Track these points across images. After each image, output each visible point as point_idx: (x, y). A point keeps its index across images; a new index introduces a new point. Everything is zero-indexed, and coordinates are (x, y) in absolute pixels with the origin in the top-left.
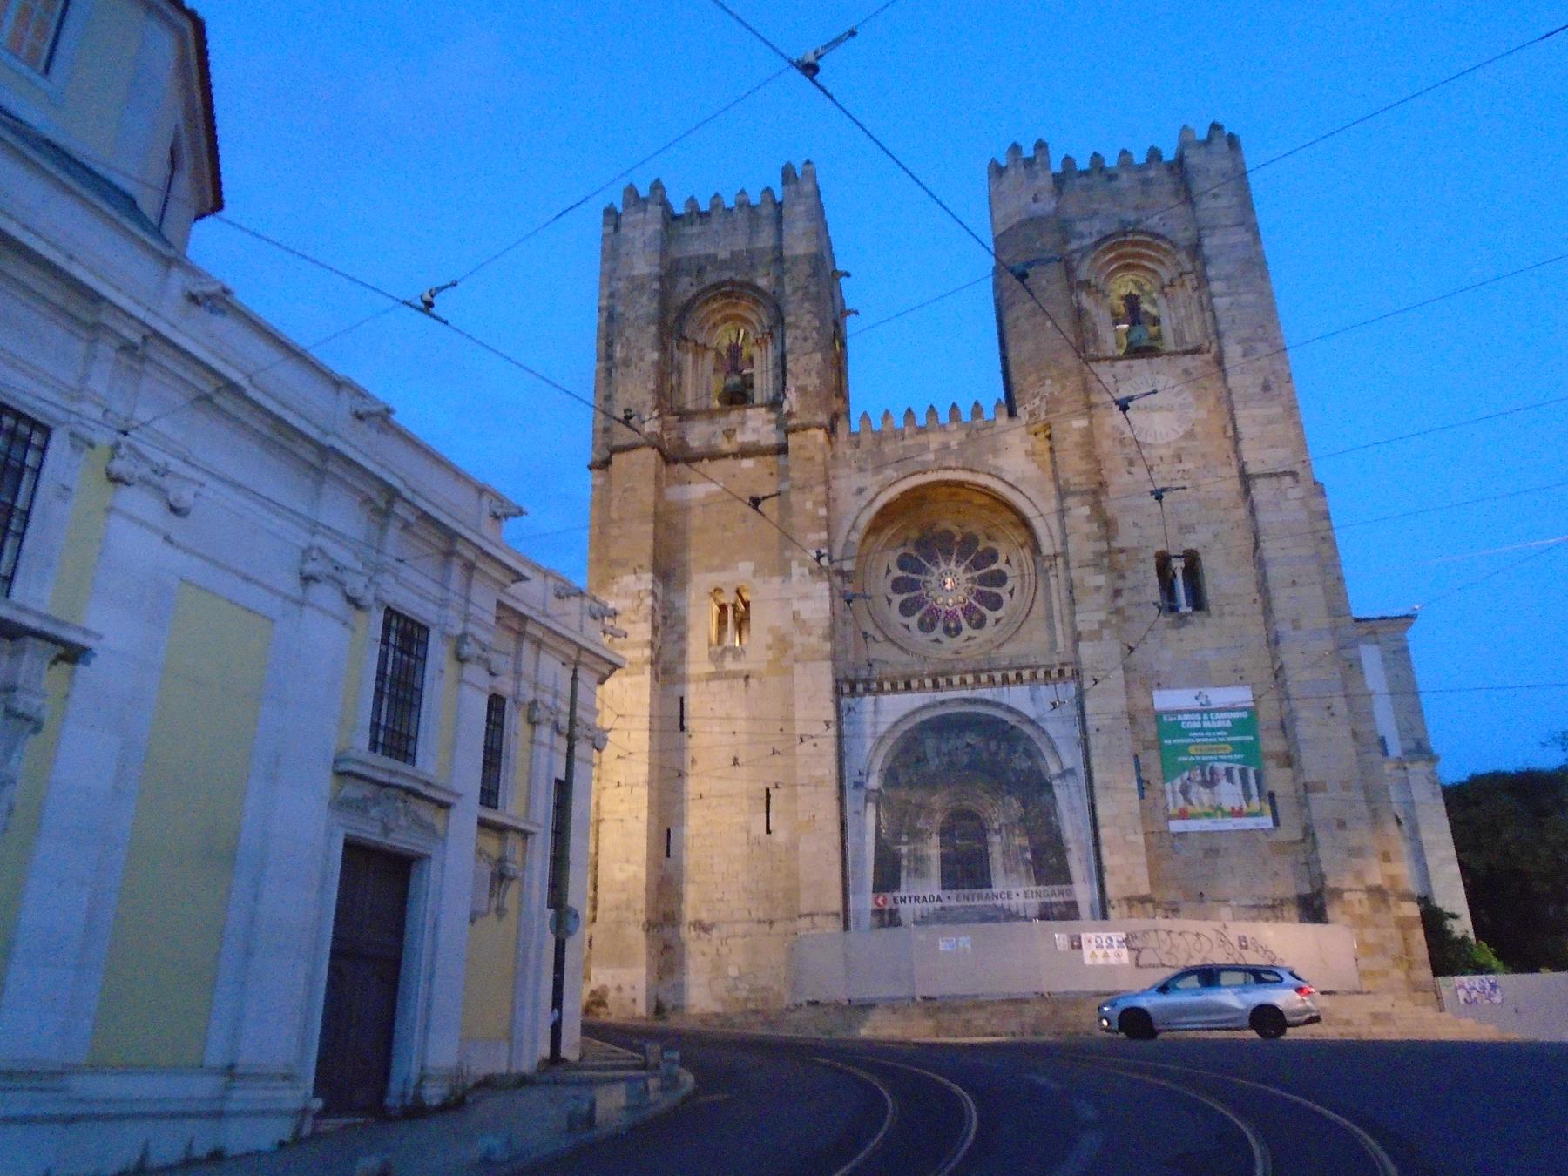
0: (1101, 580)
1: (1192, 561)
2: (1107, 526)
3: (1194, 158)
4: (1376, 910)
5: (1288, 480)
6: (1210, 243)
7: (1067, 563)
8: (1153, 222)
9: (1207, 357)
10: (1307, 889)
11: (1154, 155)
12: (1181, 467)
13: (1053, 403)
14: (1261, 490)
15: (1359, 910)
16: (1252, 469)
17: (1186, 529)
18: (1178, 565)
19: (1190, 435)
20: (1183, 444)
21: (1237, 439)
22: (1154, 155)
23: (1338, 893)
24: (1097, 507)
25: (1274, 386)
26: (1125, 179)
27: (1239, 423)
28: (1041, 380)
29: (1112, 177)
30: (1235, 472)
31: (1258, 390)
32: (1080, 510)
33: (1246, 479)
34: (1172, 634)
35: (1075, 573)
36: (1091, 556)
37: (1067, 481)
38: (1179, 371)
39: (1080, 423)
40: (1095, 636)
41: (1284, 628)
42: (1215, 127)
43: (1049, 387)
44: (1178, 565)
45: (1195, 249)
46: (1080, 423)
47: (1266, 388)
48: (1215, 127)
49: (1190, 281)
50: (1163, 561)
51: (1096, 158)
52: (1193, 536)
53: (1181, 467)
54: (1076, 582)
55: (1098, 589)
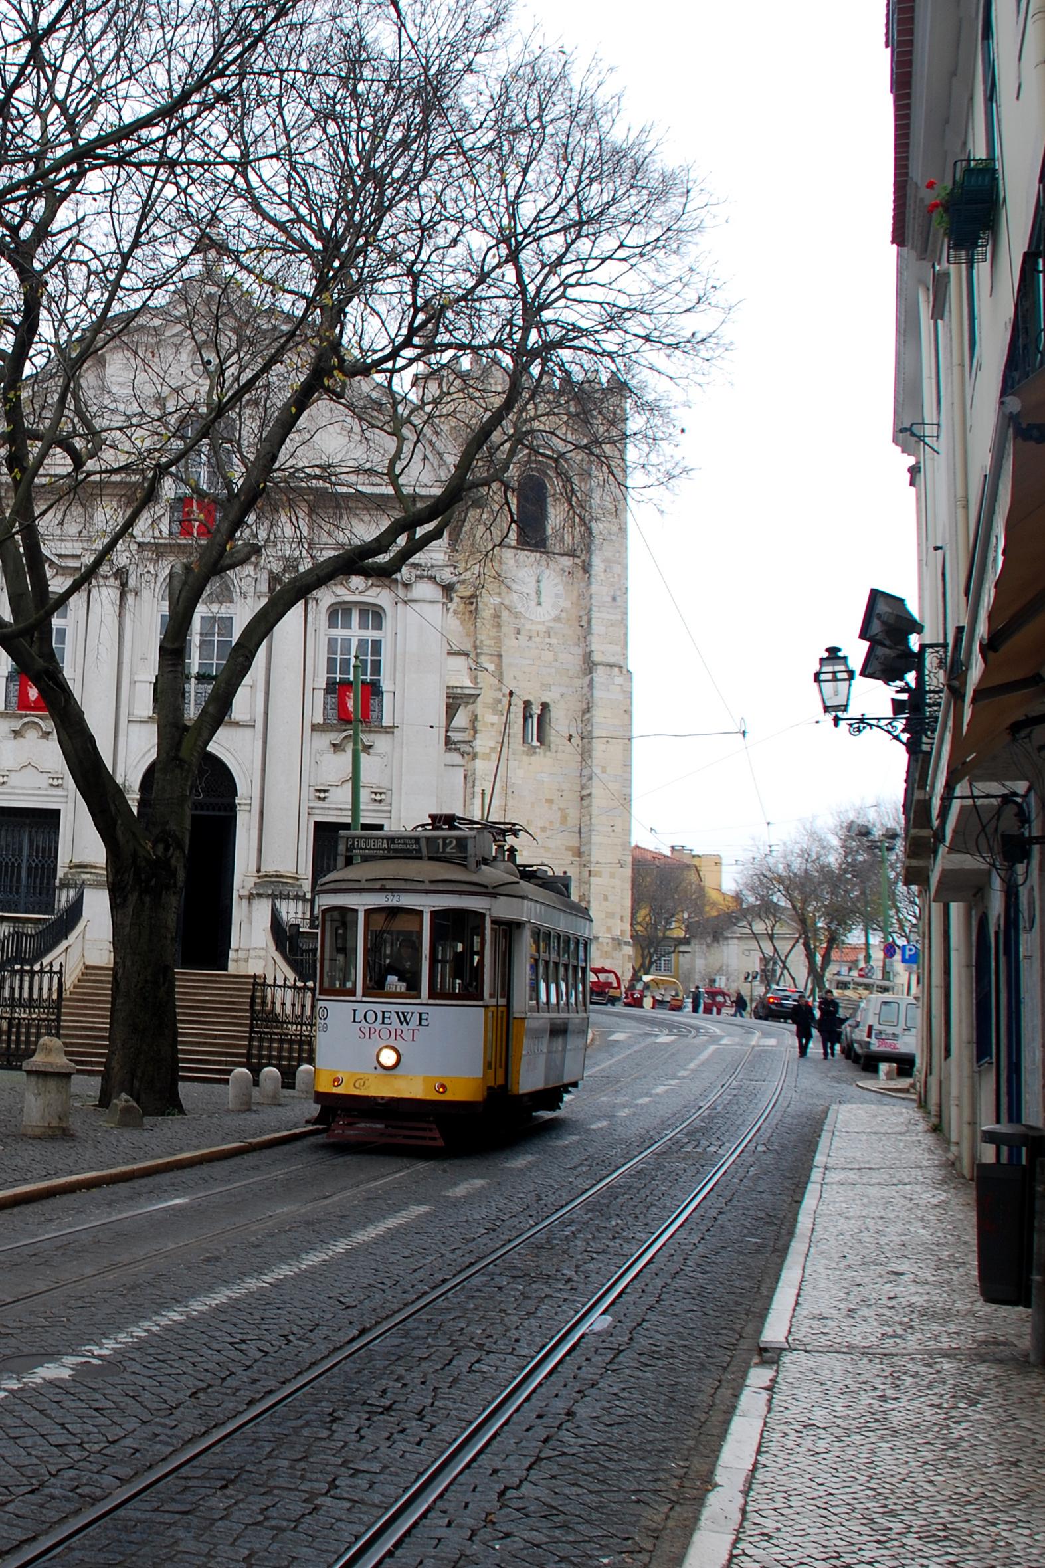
1: (545, 706)
4: (614, 949)
5: (616, 669)
9: (577, 561)
12: (548, 641)
14: (600, 675)
15: (606, 948)
16: (597, 657)
17: (546, 687)
18: (536, 710)
19: (557, 619)
20: (552, 624)
21: (585, 630)
23: (597, 938)
25: (618, 599)
27: (593, 621)
30: (579, 651)
31: (609, 599)
33: (589, 665)
34: (525, 758)
36: (491, 701)
37: (481, 642)
38: (558, 568)
41: (597, 770)
44: (536, 710)
47: (614, 599)
50: (527, 704)
52: (549, 693)
53: (548, 641)
54: (479, 718)
55: (493, 724)
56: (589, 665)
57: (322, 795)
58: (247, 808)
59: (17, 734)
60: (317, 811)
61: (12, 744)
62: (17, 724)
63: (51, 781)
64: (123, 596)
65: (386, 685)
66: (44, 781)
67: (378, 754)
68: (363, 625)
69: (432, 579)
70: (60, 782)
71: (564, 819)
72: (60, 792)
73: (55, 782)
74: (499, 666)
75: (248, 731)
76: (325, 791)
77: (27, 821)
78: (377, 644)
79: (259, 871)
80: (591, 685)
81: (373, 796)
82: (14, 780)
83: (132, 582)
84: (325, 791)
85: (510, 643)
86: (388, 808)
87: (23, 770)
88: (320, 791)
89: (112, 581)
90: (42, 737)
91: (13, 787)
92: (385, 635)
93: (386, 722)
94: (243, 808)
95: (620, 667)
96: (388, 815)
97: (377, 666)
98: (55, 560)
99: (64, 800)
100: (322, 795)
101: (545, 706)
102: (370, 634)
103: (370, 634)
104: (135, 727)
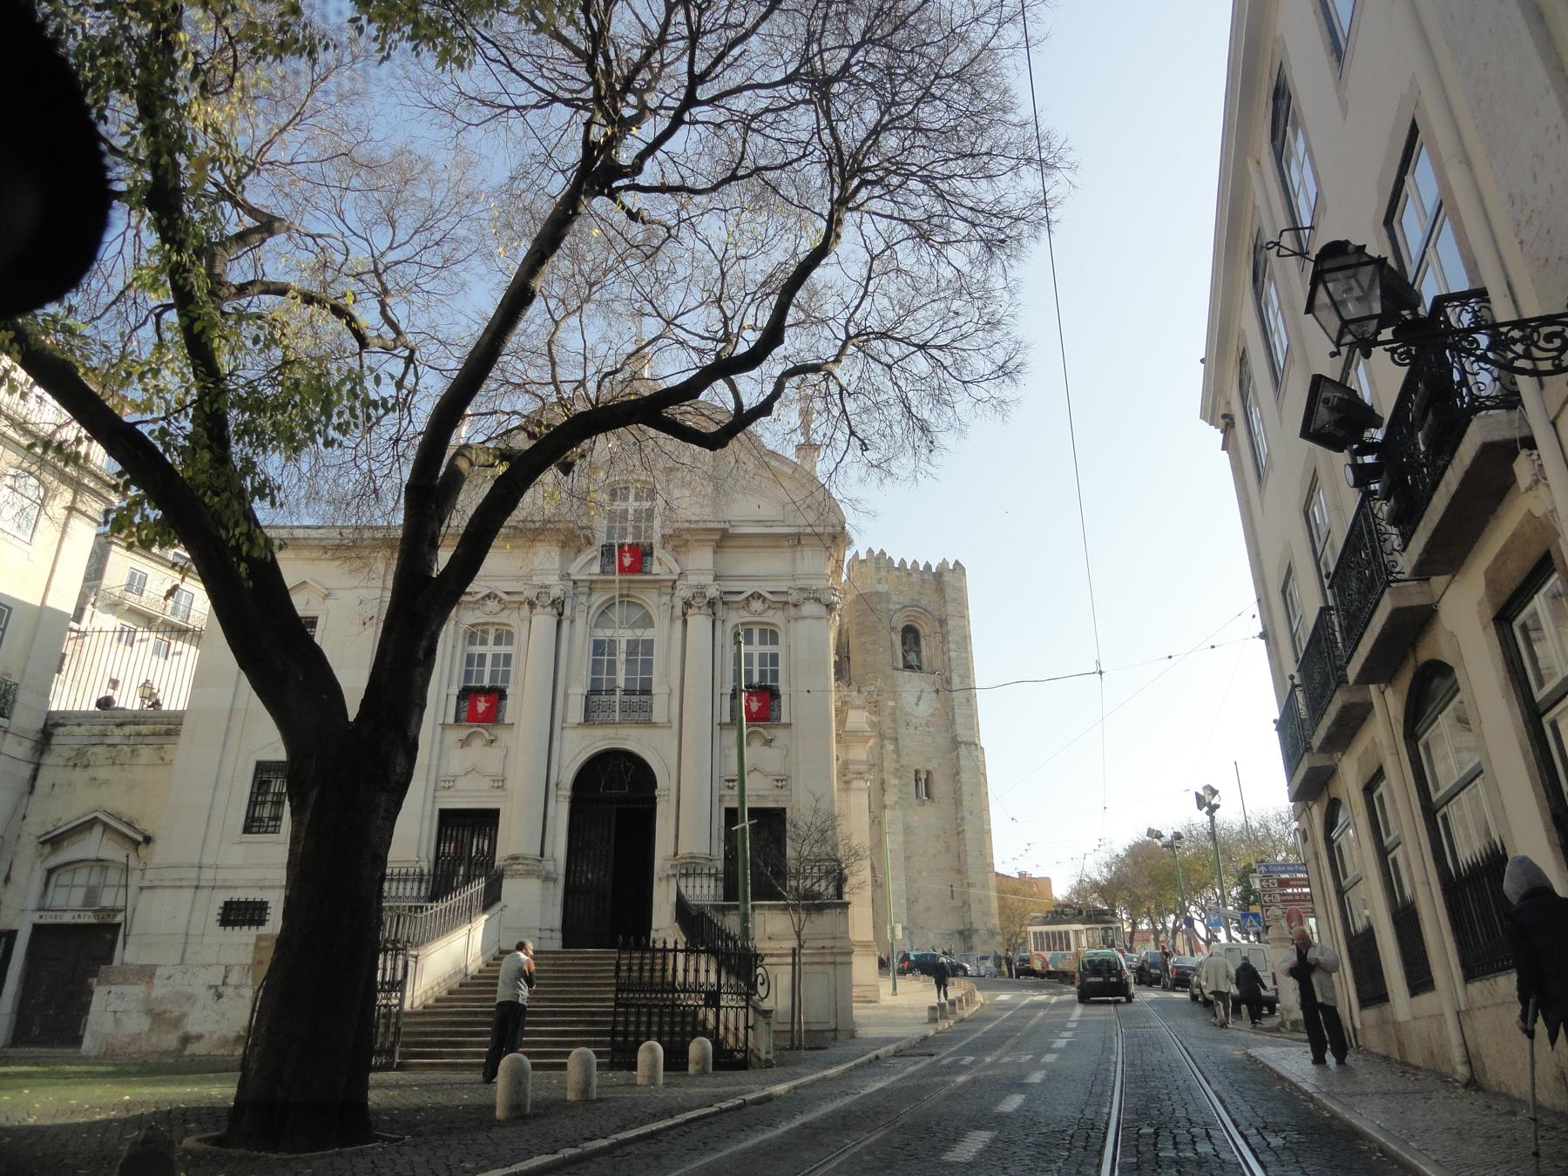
0: (896, 782)
2: (897, 751)
3: (947, 578)
6: (951, 623)
7: (881, 771)
8: (923, 603)
10: (961, 927)
11: (928, 566)
13: (880, 692)
14: (963, 750)
19: (932, 715)
22: (928, 566)
24: (897, 745)
26: (915, 576)
28: (876, 678)
29: (909, 575)
32: (890, 747)
35: (886, 777)
39: (891, 703)
40: (893, 808)
41: (966, 814)
42: (957, 563)
43: (879, 683)
44: (923, 776)
45: (942, 622)
46: (891, 703)
48: (957, 563)
49: (939, 637)
50: (917, 772)
51: (903, 562)
56: (955, 744)
59: (465, 743)
62: (463, 733)
64: (559, 623)
65: (783, 689)
66: (487, 783)
68: (763, 642)
69: (818, 600)
71: (948, 849)
72: (499, 793)
74: (897, 745)
78: (774, 658)
80: (958, 757)
82: (461, 783)
83: (567, 612)
85: (903, 731)
92: (779, 649)
93: (784, 720)
95: (974, 745)
97: (775, 674)
98: (504, 596)
101: (928, 773)
102: (768, 649)
103: (768, 649)
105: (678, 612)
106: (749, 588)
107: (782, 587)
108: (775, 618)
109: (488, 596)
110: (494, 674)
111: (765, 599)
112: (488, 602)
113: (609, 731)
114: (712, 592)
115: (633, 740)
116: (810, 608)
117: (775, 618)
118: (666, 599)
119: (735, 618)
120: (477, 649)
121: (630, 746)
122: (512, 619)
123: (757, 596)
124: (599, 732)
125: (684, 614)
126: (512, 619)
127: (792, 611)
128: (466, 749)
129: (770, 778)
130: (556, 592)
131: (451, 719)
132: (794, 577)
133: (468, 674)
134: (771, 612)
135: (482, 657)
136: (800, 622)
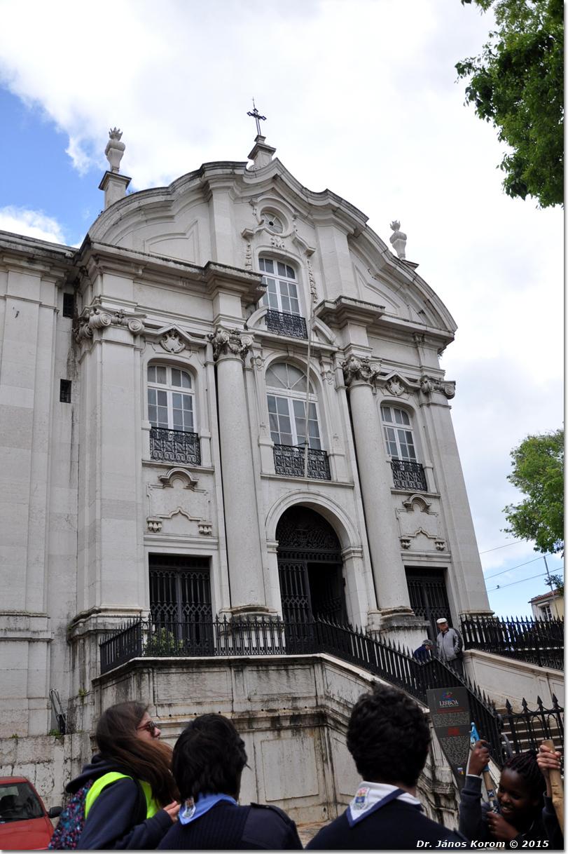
57: (407, 544)
58: (360, 555)
59: (165, 483)
60: (405, 558)
61: (160, 493)
63: (201, 529)
65: (427, 464)
67: (434, 514)
70: (210, 530)
73: (206, 530)
75: (349, 492)
76: (408, 541)
77: (179, 569)
79: (378, 608)
81: (438, 545)
82: (167, 527)
84: (408, 541)
86: (449, 555)
87: (174, 519)
88: (405, 541)
89: (239, 357)
90: (188, 488)
91: (168, 535)
94: (356, 555)
96: (448, 560)
99: (215, 547)
100: (407, 544)
104: (266, 484)
105: (342, 382)
106: (391, 371)
107: (416, 375)
108: (410, 400)
109: (169, 332)
110: (177, 413)
111: (402, 383)
112: (169, 339)
113: (304, 488)
114: (376, 368)
115: (323, 497)
116: (437, 397)
117: (410, 400)
118: (327, 368)
119: (383, 395)
120: (157, 385)
121: (321, 501)
122: (193, 359)
123: (396, 379)
124: (294, 487)
125: (346, 385)
126: (193, 359)
127: (423, 399)
128: (169, 490)
129: (432, 542)
130: (248, 340)
131: (148, 457)
132: (421, 369)
133: (152, 411)
134: (405, 396)
135: (163, 395)
136: (432, 407)
